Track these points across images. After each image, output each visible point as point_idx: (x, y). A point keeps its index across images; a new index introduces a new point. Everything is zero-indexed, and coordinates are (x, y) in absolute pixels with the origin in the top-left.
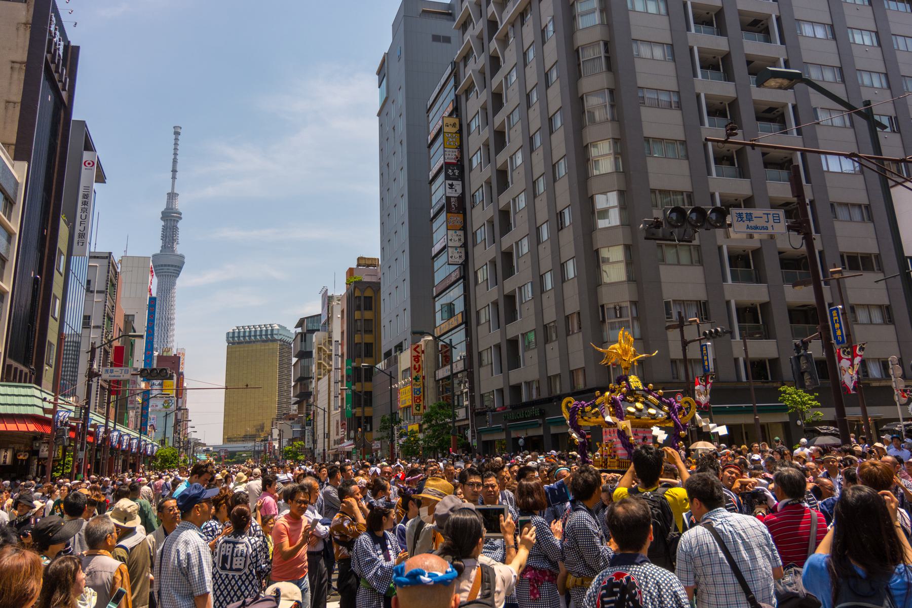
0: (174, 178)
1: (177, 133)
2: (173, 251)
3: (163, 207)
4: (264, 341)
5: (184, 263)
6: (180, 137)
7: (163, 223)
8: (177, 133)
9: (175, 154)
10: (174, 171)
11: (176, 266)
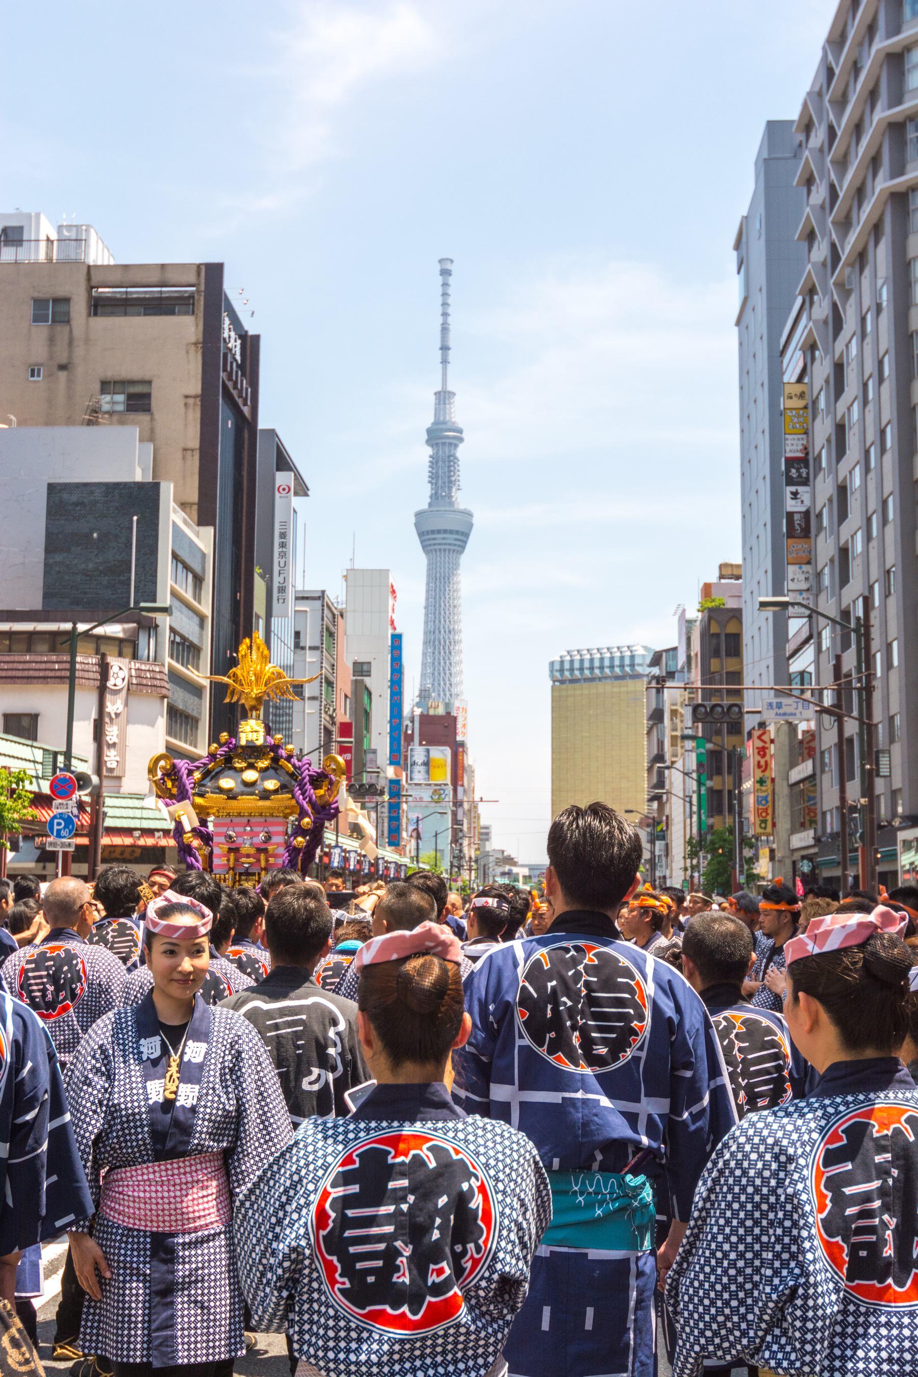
0: (445, 361)
1: (445, 273)
2: (451, 504)
3: (428, 420)
4: (617, 678)
5: (471, 525)
6: (451, 280)
7: (429, 451)
8: (445, 273)
9: (445, 315)
10: (445, 348)
11: (457, 532)
